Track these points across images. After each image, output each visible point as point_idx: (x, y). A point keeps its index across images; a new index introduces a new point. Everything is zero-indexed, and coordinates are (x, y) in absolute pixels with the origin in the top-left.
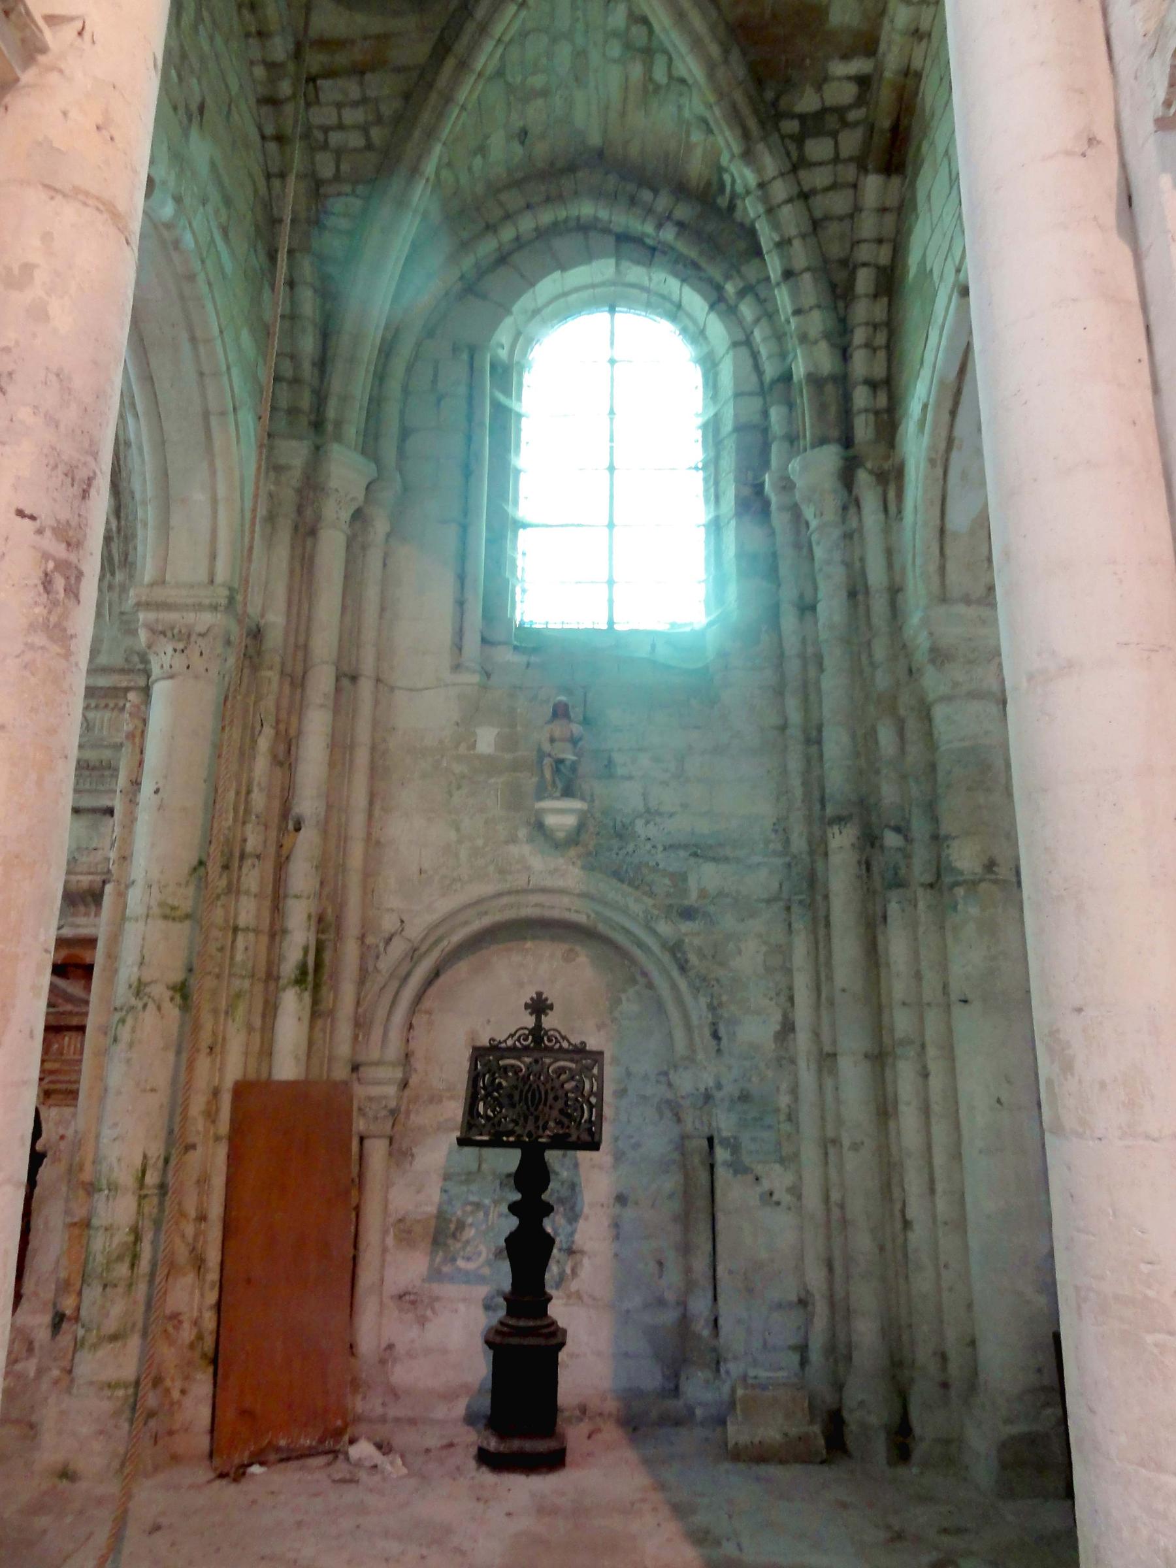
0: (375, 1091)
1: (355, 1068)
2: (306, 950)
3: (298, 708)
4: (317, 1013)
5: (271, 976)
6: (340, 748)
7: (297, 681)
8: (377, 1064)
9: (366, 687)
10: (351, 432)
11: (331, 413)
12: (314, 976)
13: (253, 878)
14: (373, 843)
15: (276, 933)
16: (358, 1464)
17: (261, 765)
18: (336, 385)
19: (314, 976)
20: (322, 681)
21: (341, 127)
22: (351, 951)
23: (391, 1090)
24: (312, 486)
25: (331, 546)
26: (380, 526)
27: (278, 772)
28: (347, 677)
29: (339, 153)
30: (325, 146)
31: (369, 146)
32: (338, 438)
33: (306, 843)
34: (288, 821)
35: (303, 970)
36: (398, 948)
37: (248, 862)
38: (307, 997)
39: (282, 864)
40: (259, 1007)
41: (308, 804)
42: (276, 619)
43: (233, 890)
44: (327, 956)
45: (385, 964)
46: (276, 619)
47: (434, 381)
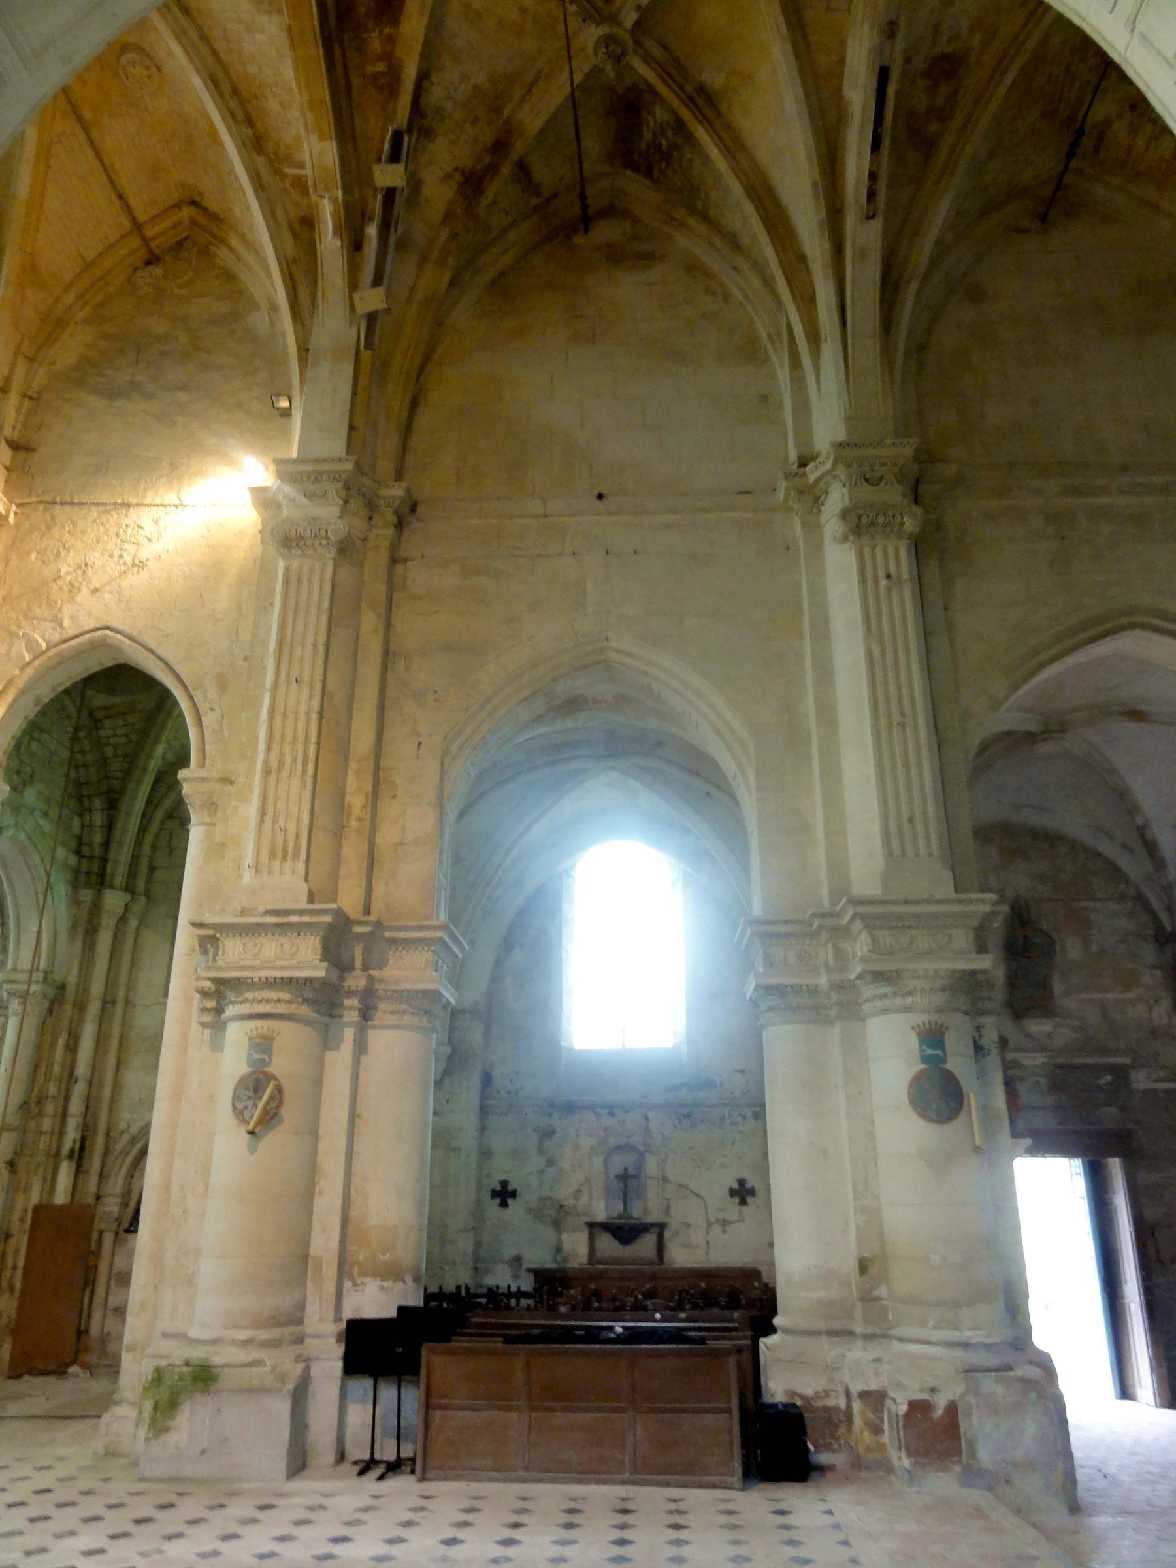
0: (108, 1209)
1: (98, 1198)
2: (74, 1142)
3: (81, 1021)
4: (79, 1171)
5: (58, 1154)
6: (101, 1039)
7: (81, 1007)
8: (110, 1195)
9: (119, 1009)
10: (118, 880)
11: (109, 871)
12: (80, 1155)
13: (50, 1108)
14: (117, 1086)
15: (62, 1134)
16: (72, 1375)
17: (59, 1053)
18: (112, 856)
19: (80, 1155)
20: (94, 1008)
21: (115, 735)
22: (100, 1142)
23: (116, 1209)
24: (96, 908)
25: (104, 939)
26: (133, 923)
27: (69, 1055)
28: (108, 1002)
29: (115, 747)
30: (108, 744)
31: (130, 741)
32: (112, 887)
33: (79, 1089)
34: (71, 1078)
35: (72, 1152)
36: (126, 1138)
37: (50, 1100)
38: (73, 1165)
39: (67, 1099)
40: (50, 1170)
41: (82, 1070)
42: (73, 979)
43: (41, 1114)
44: (87, 1143)
45: (119, 1146)
46: (73, 979)
47: (170, 842)
